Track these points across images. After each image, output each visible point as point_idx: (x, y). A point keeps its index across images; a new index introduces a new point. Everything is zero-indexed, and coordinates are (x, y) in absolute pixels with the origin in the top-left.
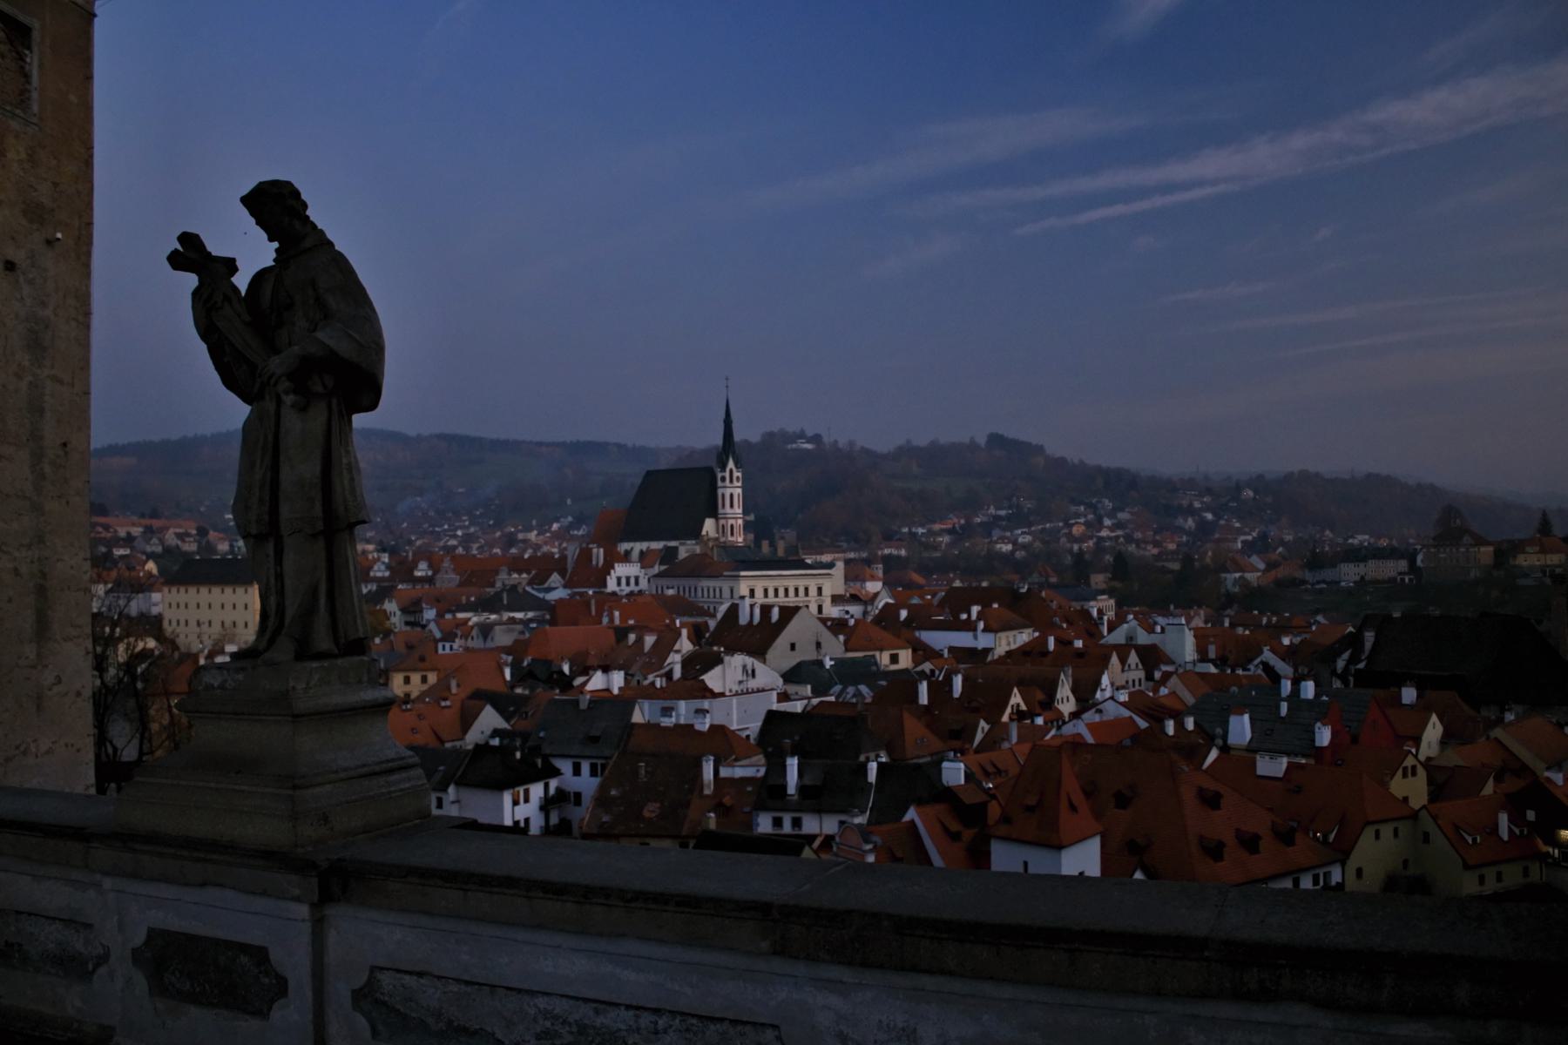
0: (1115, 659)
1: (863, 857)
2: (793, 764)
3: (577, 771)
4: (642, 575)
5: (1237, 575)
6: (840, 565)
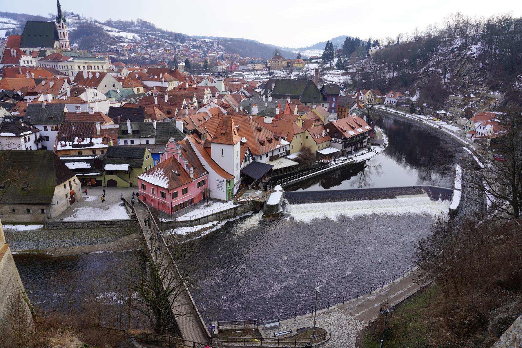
2: (129, 123)
3: (46, 129)
5: (221, 67)
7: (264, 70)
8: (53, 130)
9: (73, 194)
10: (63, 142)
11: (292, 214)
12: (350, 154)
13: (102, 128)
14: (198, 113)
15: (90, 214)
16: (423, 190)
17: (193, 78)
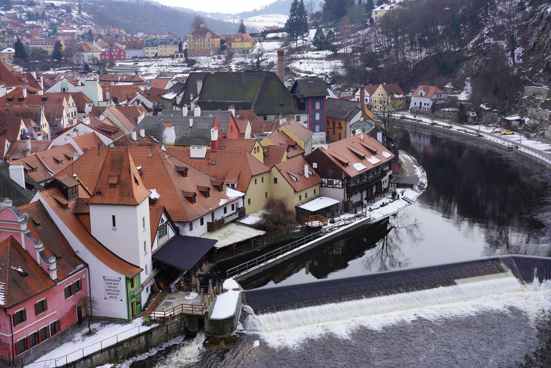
0: (65, 100)
1: (19, 226)
5: (90, 54)
7: (177, 56)
11: (264, 335)
12: (360, 208)
14: (53, 147)
16: (502, 264)
17: (35, 77)
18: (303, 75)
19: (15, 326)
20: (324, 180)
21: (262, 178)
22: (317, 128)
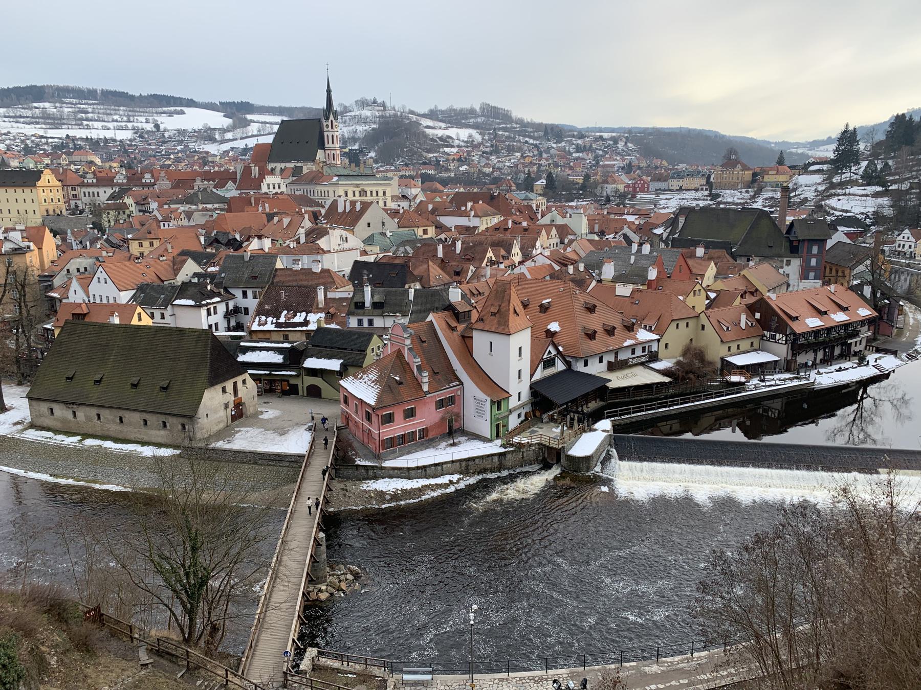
0: (544, 232)
2: (368, 290)
3: (245, 295)
4: (282, 183)
5: (613, 186)
6: (396, 178)
7: (702, 189)
8: (255, 297)
9: (238, 405)
10: (263, 318)
12: (804, 370)
13: (329, 297)
15: (255, 440)
17: (535, 209)
18: (838, 213)
19: (382, 424)
20: (765, 332)
21: (687, 323)
22: (812, 274)
